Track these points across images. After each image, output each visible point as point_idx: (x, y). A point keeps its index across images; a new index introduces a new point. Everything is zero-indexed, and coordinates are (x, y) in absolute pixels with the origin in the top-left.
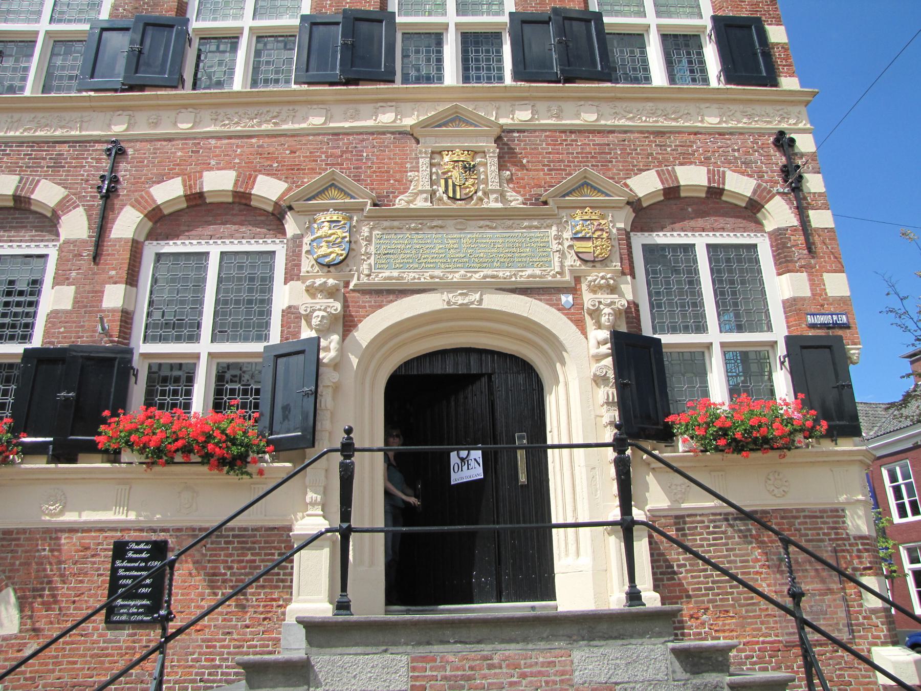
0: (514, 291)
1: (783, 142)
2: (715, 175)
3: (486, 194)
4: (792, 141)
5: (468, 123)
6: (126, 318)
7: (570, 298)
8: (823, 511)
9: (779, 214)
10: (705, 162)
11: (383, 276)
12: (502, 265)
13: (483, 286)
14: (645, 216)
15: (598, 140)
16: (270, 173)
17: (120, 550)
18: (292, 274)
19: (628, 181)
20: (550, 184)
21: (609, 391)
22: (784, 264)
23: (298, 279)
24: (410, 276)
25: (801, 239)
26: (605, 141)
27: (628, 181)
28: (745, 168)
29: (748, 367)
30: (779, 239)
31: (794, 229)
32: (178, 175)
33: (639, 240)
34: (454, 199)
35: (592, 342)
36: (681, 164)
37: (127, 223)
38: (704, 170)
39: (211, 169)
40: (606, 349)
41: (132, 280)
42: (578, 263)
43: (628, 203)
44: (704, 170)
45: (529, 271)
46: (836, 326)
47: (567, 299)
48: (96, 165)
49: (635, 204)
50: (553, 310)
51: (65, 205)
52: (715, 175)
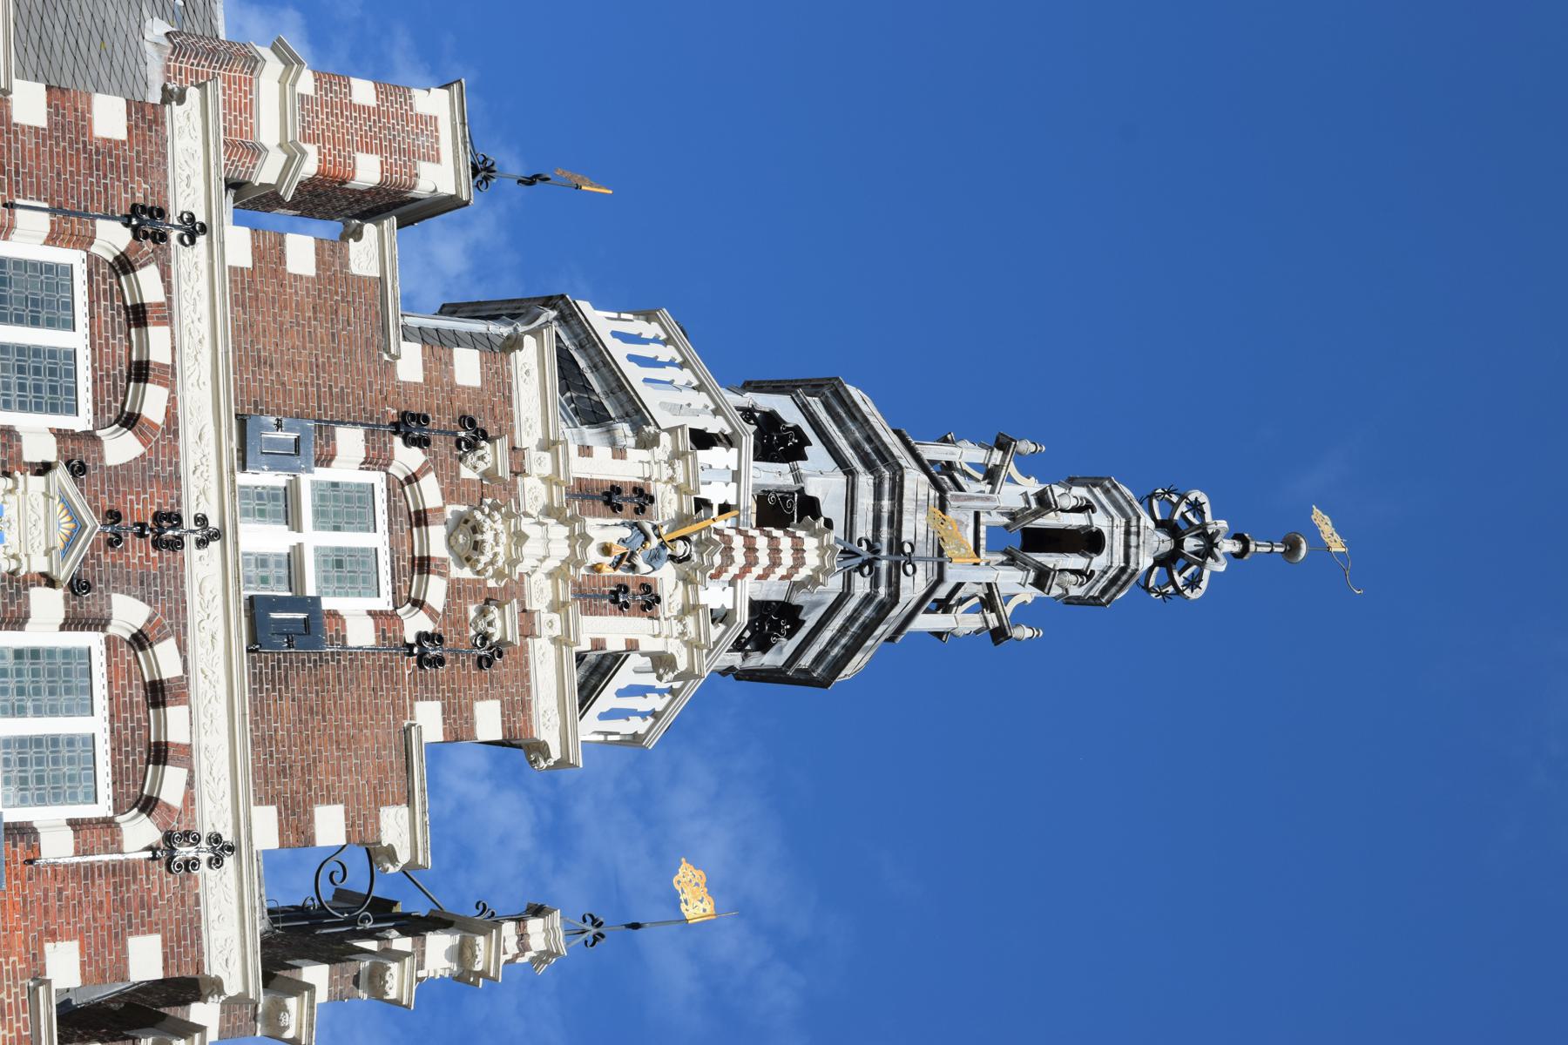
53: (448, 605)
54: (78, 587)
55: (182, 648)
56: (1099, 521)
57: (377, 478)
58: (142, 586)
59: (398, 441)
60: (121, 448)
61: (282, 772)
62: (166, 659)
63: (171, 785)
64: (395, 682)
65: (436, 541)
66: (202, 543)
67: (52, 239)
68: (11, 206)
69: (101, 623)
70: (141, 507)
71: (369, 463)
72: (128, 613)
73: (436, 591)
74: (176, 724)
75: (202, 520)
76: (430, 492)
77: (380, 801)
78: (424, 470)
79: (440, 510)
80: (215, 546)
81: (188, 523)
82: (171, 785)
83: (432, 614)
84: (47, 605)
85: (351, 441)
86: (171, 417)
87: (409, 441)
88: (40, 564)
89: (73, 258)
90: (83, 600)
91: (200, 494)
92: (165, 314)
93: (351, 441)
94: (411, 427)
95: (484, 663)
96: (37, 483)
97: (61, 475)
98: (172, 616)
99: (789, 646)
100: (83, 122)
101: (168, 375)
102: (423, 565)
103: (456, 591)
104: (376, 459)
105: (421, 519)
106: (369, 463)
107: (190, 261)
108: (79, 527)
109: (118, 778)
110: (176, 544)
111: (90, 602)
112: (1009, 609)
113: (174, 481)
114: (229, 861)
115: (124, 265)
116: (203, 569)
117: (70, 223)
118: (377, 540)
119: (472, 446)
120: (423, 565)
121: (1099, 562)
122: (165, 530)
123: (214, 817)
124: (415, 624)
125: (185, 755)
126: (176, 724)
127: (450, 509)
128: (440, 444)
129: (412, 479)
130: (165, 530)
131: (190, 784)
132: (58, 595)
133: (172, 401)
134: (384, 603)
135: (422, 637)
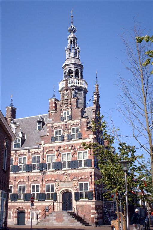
1: (91, 173)
6: (45, 190)
9: (90, 180)
13: (67, 187)
16: (53, 178)
17: (46, 207)
20: (74, 178)
24: (63, 187)
33: (79, 183)
37: (44, 182)
41: (45, 187)
47: (73, 188)
54: (69, 130)
56: (70, 41)
58: (68, 126)
60: (62, 128)
67: (54, 132)
72: (70, 127)
92: (56, 126)
98: (70, 124)
99: (78, 69)
100: (48, 131)
101: (59, 125)
109: (78, 126)
111: (69, 129)
112: (77, 48)
116: (68, 122)
117: (53, 131)
121: (73, 40)
123: (79, 121)
124: (70, 109)
130: (66, 125)
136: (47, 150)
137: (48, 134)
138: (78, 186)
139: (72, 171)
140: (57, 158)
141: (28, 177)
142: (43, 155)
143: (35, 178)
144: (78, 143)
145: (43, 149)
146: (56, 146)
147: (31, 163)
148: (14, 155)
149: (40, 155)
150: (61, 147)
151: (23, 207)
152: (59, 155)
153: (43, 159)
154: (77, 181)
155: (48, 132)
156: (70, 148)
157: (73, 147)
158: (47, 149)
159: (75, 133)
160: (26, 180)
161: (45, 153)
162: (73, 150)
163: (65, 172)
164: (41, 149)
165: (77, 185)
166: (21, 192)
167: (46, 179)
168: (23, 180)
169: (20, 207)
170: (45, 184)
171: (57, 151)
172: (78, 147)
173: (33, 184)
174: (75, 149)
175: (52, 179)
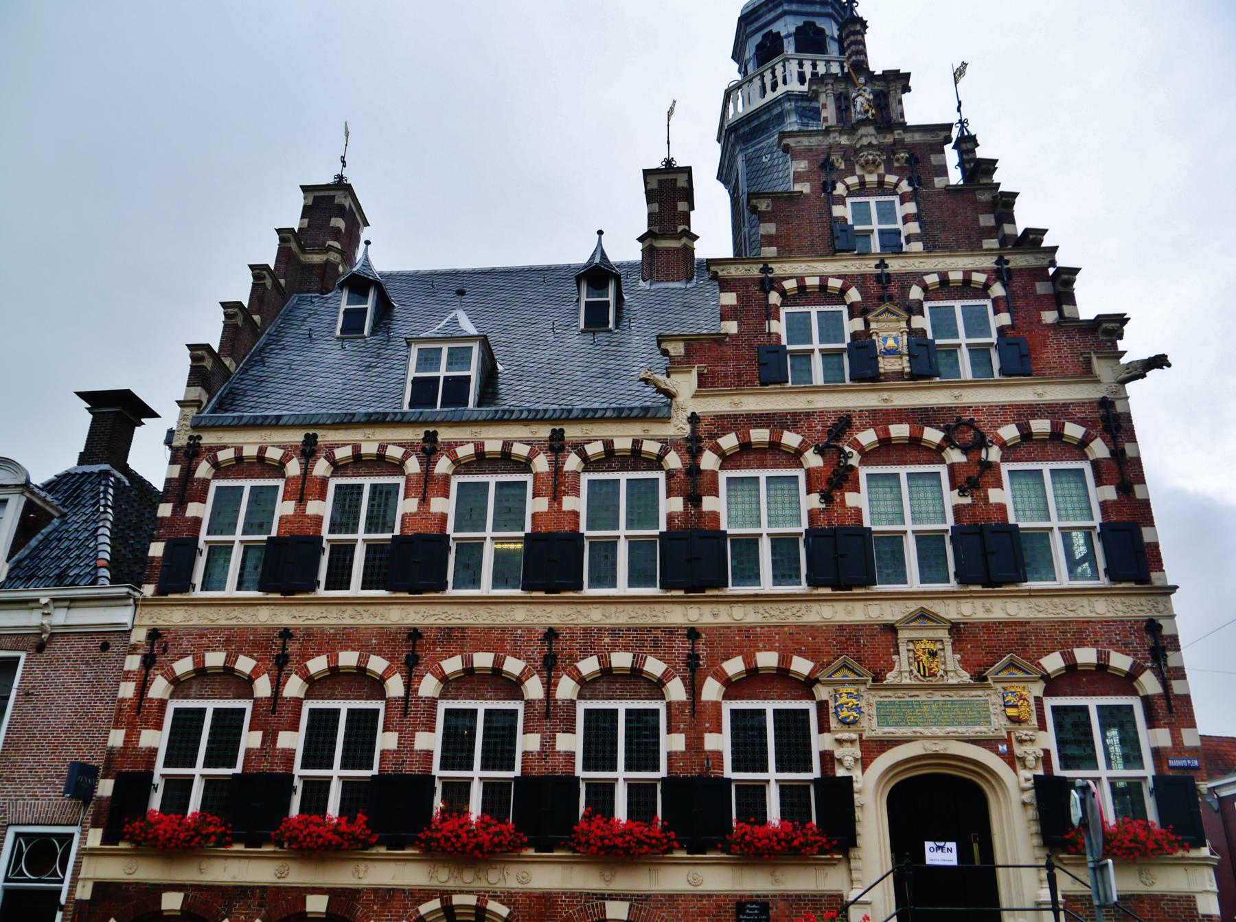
0: (967, 741)
2: (1103, 657)
3: (946, 672)
4: (1161, 626)
5: (930, 619)
7: (1005, 747)
8: (1180, 897)
9: (1149, 683)
10: (1095, 644)
11: (881, 732)
12: (960, 724)
14: (1053, 685)
15: (1019, 629)
16: (800, 654)
18: (824, 728)
19: (1041, 661)
21: (1032, 813)
22: (1152, 723)
23: (829, 731)
25: (1162, 703)
26: (1023, 629)
27: (1041, 661)
28: (1124, 648)
29: (1127, 794)
30: (1147, 701)
31: (1159, 696)
32: (738, 654)
33: (1049, 703)
34: (924, 676)
35: (1022, 779)
36: (1078, 646)
37: (711, 690)
38: (1094, 651)
39: (760, 650)
40: (1029, 784)
41: (719, 730)
42: (1008, 723)
43: (1042, 678)
44: (1094, 651)
45: (978, 729)
46: (1188, 768)
48: (681, 646)
49: (1046, 677)
50: (994, 755)
51: (667, 676)
52: (1103, 657)
53: (896, 174)
55: (927, 274)
57: (849, 201)
58: (905, 290)
59: (835, 193)
60: (854, 295)
61: (969, 238)
62: (932, 279)
63: (979, 278)
64: (929, 195)
65: (871, 178)
66: (886, 266)
68: (770, 334)
69: (920, 303)
70: (874, 288)
71: (844, 204)
72: (916, 293)
73: (891, 179)
74: (956, 276)
75: (877, 266)
76: (852, 180)
77: (975, 201)
78: (844, 183)
79: (879, 176)
80: (887, 262)
81: (879, 271)
82: (979, 278)
83: (900, 181)
84: (918, 322)
85: (837, 211)
86: (839, 277)
87: (834, 188)
88: (903, 324)
89: (783, 311)
90: (914, 309)
91: (868, 266)
92: (800, 279)
93: (837, 211)
94: (828, 187)
95: (917, 161)
96: (873, 326)
97: (869, 317)
98: (917, 277)
101: (824, 278)
102: (881, 183)
103: (889, 171)
104: (841, 201)
105: (862, 183)
106: (844, 204)
107: (779, 269)
108: (887, 311)
110: (888, 275)
113: (864, 276)
114: (1006, 258)
115: (783, 293)
118: (872, 201)
119: (832, 164)
120: (881, 183)
122: (883, 279)
123: (989, 262)
124: (905, 187)
125: (967, 273)
126: (956, 276)
127: (859, 171)
128: (834, 176)
129: (848, 187)
131: (977, 271)
132: (913, 318)
133: (833, 276)
134: (896, 199)
135: (910, 184)
136: (729, 442)
137: (731, 327)
138: (1042, 726)
139: (978, 603)
140: (827, 498)
141: (551, 634)
142: (693, 470)
143: (614, 647)
144: (1003, 407)
145: (687, 430)
146: (809, 415)
147: (577, 524)
148: (406, 456)
149: (661, 476)
150: (856, 421)
151: (493, 906)
152: (837, 479)
153: (694, 500)
154: (1037, 689)
155: (727, 314)
156: (933, 435)
157: (965, 430)
158: (725, 431)
159: (963, 339)
160: (527, 659)
161: (709, 461)
162: (965, 450)
163: (923, 615)
164: (678, 428)
165: (1034, 721)
166: (470, 767)
167: (727, 658)
168: (498, 662)
169: (457, 900)
170: (717, 706)
171: (820, 451)
172: (1009, 432)
173: (593, 697)
174: (981, 442)
175: (785, 659)
